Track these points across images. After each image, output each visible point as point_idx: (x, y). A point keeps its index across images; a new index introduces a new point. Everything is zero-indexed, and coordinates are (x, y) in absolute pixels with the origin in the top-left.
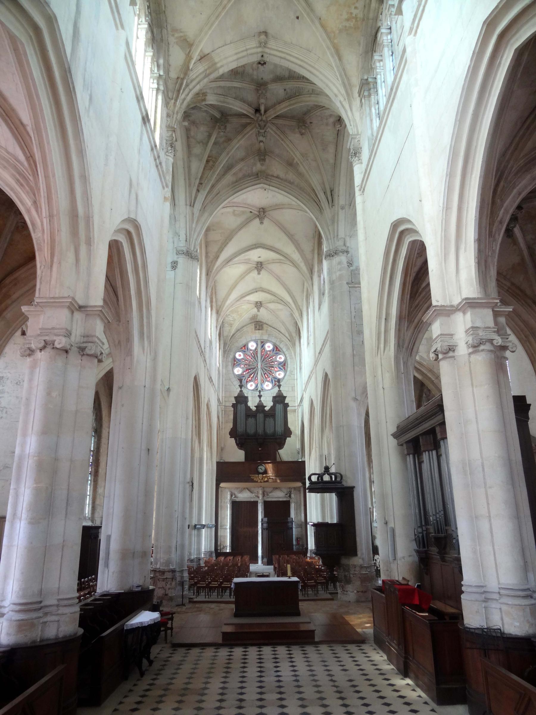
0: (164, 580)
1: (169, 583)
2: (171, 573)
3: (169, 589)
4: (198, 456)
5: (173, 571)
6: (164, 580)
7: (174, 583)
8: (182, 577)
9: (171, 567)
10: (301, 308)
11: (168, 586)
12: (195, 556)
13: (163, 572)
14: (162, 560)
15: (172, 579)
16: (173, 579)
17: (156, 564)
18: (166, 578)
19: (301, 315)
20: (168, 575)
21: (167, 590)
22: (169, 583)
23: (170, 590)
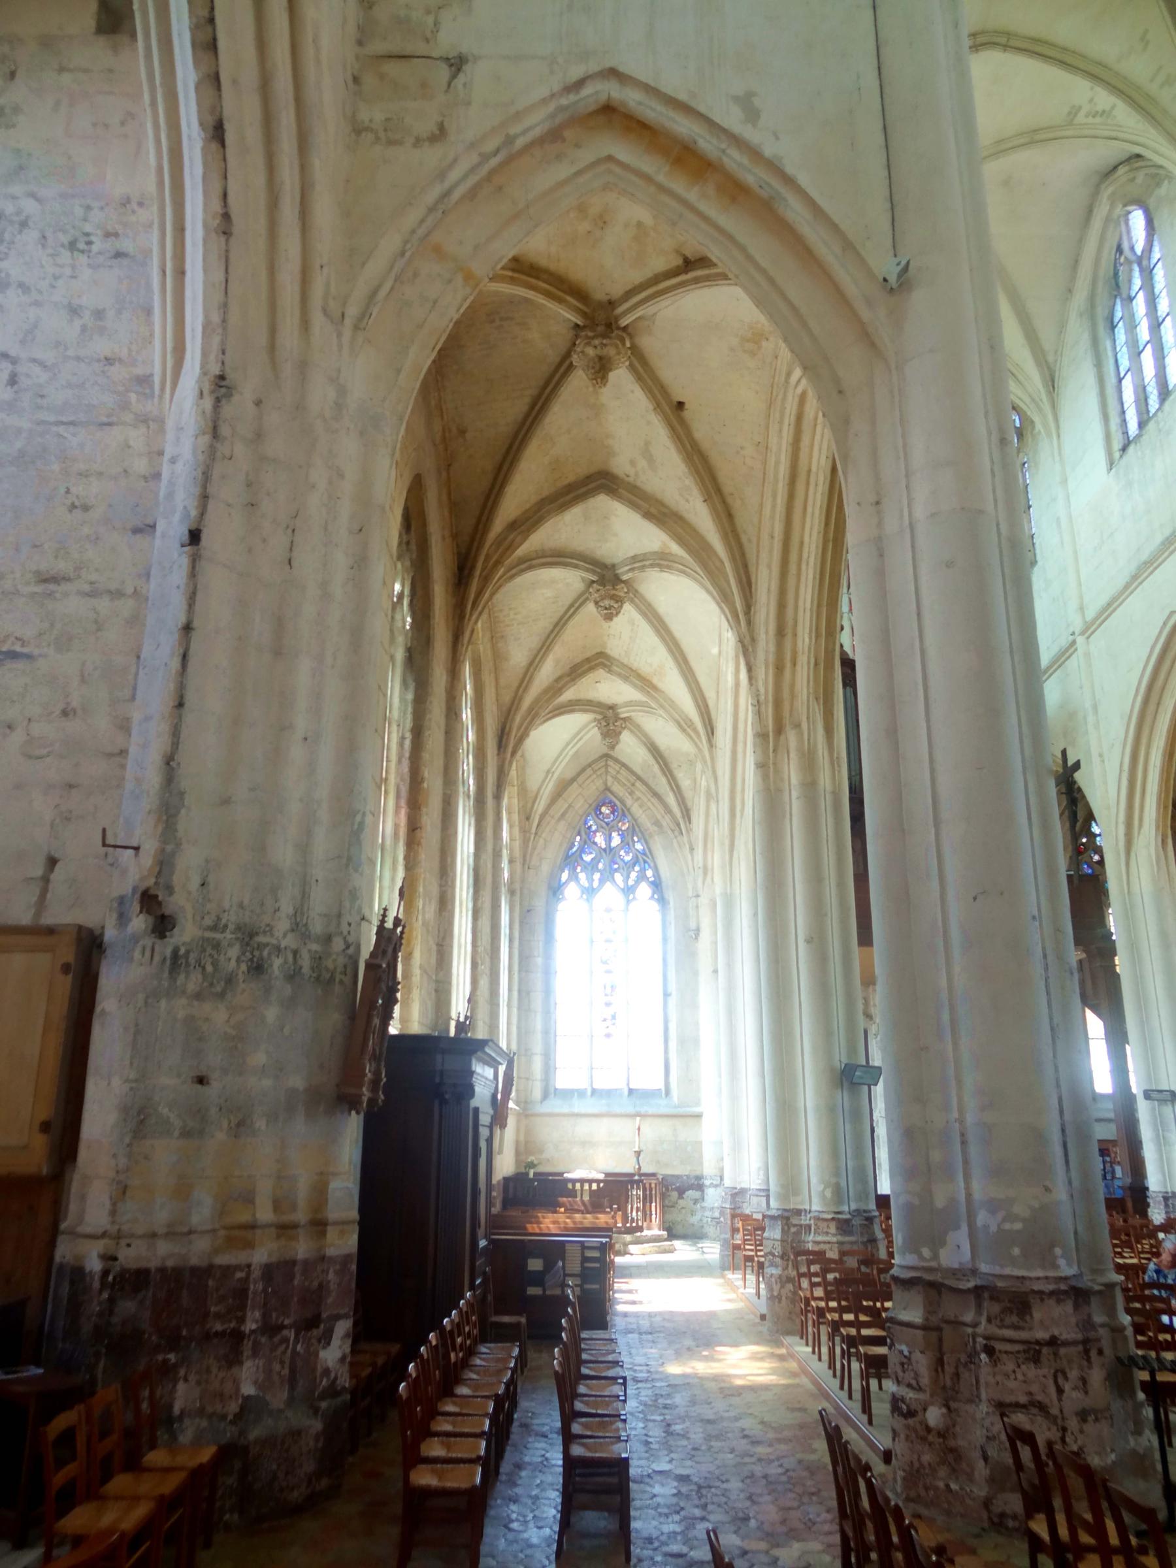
0: (1033, 1353)
1: (1074, 1374)
2: (1069, 1306)
3: (1083, 1415)
4: (829, 788)
5: (1078, 1295)
6: (1033, 1353)
7: (1097, 1376)
8: (1118, 1330)
9: (1067, 1269)
10: (1051, 359)
11: (1073, 1398)
12: (853, 1206)
13: (1018, 1302)
14: (982, 1218)
15: (1085, 1342)
16: (1087, 1345)
17: (936, 1242)
18: (1053, 1342)
19: (1052, 382)
20: (1053, 1321)
21: (1073, 1424)
22: (1074, 1374)
23: (1090, 1427)
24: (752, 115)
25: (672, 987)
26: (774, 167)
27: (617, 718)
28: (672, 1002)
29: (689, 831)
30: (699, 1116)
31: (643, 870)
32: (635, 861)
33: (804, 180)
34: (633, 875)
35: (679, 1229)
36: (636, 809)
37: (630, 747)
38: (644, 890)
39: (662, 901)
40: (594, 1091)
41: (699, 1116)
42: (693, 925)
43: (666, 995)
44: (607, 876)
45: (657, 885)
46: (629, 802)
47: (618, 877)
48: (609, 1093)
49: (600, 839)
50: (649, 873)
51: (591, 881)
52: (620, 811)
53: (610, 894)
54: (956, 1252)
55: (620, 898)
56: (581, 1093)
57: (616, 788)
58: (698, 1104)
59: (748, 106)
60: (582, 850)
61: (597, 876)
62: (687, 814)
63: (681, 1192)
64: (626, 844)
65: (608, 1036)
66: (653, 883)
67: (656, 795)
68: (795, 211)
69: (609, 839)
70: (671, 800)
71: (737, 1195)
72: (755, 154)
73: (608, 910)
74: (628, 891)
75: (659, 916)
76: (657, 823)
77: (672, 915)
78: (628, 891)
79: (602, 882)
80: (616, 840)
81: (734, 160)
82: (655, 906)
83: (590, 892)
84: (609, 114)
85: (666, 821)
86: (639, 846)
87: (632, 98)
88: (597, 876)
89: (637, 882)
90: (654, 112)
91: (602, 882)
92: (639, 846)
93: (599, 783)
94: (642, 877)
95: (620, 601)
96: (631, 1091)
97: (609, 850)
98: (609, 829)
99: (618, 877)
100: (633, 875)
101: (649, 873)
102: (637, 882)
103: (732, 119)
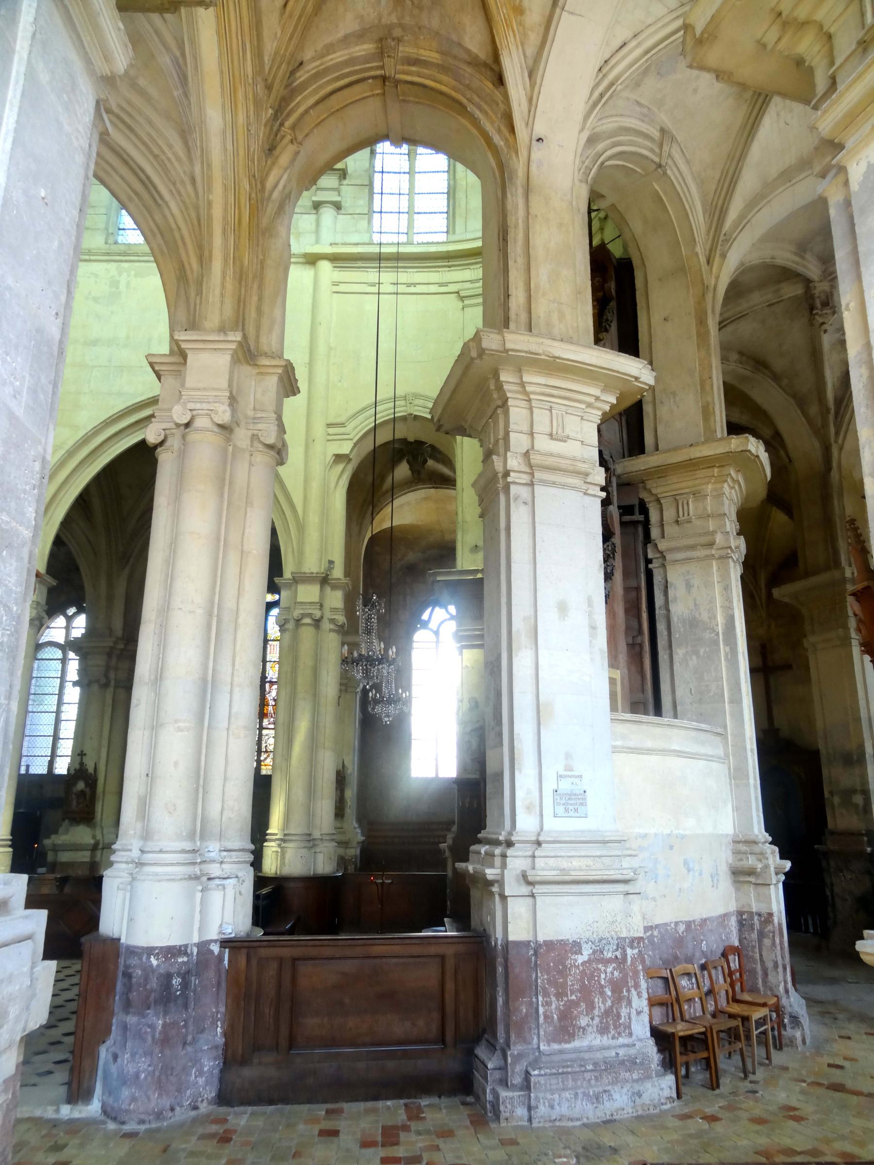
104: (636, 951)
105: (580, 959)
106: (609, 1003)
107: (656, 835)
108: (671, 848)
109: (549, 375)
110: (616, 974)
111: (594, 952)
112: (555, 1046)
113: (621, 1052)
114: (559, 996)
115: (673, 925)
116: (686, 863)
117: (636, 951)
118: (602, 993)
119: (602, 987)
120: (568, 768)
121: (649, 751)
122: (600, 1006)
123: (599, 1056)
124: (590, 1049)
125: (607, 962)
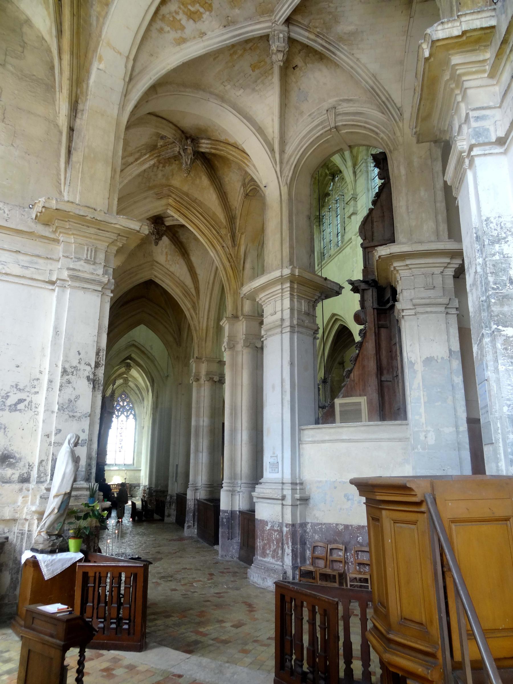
24: (152, 349)
25: (137, 440)
26: (154, 356)
27: (128, 380)
28: (136, 444)
29: (143, 403)
30: (140, 470)
31: (131, 412)
32: (130, 409)
33: (157, 359)
34: (129, 413)
35: (133, 496)
36: (131, 396)
37: (130, 384)
38: (131, 416)
39: (136, 419)
40: (116, 464)
41: (140, 470)
42: (142, 425)
43: (135, 442)
44: (122, 413)
45: (135, 415)
46: (129, 394)
47: (125, 413)
48: (119, 465)
49: (121, 403)
50: (133, 412)
51: (118, 413)
52: (127, 396)
53: (123, 417)
54: (159, 488)
55: (125, 418)
56: (112, 465)
57: (126, 391)
58: (140, 467)
59: (151, 347)
60: (116, 406)
61: (120, 413)
62: (143, 399)
63: (135, 487)
64: (128, 405)
65: (120, 451)
66: (133, 415)
67: (136, 393)
68: (156, 363)
69: (123, 404)
70: (139, 395)
71: (145, 486)
72: (152, 355)
73: (122, 421)
74: (127, 417)
75: (134, 423)
76: (136, 401)
77: (138, 423)
78: (127, 417)
79: (121, 414)
80: (125, 404)
81: (149, 355)
82: (134, 420)
83: (118, 416)
84: (134, 345)
85: (138, 400)
86: (131, 405)
87: (136, 344)
88: (120, 413)
89: (130, 414)
90: (140, 346)
91: (121, 414)
92: (131, 405)
93: (122, 390)
94: (131, 413)
95: (130, 370)
96: (125, 464)
97: (123, 407)
98: (123, 401)
99: (125, 413)
100: (129, 413)
101: (133, 412)
102: (130, 414)
103: (149, 349)
104: (288, 529)
105: (268, 528)
106: (275, 547)
107: (326, 481)
108: (335, 488)
109: (264, 291)
110: (278, 536)
111: (271, 526)
112: (261, 558)
113: (276, 567)
114: (263, 540)
115: (334, 525)
116: (345, 496)
117: (288, 529)
118: (273, 543)
119: (273, 540)
120: (274, 453)
121: (323, 442)
122: (273, 547)
123: (269, 565)
124: (269, 562)
125: (275, 531)
